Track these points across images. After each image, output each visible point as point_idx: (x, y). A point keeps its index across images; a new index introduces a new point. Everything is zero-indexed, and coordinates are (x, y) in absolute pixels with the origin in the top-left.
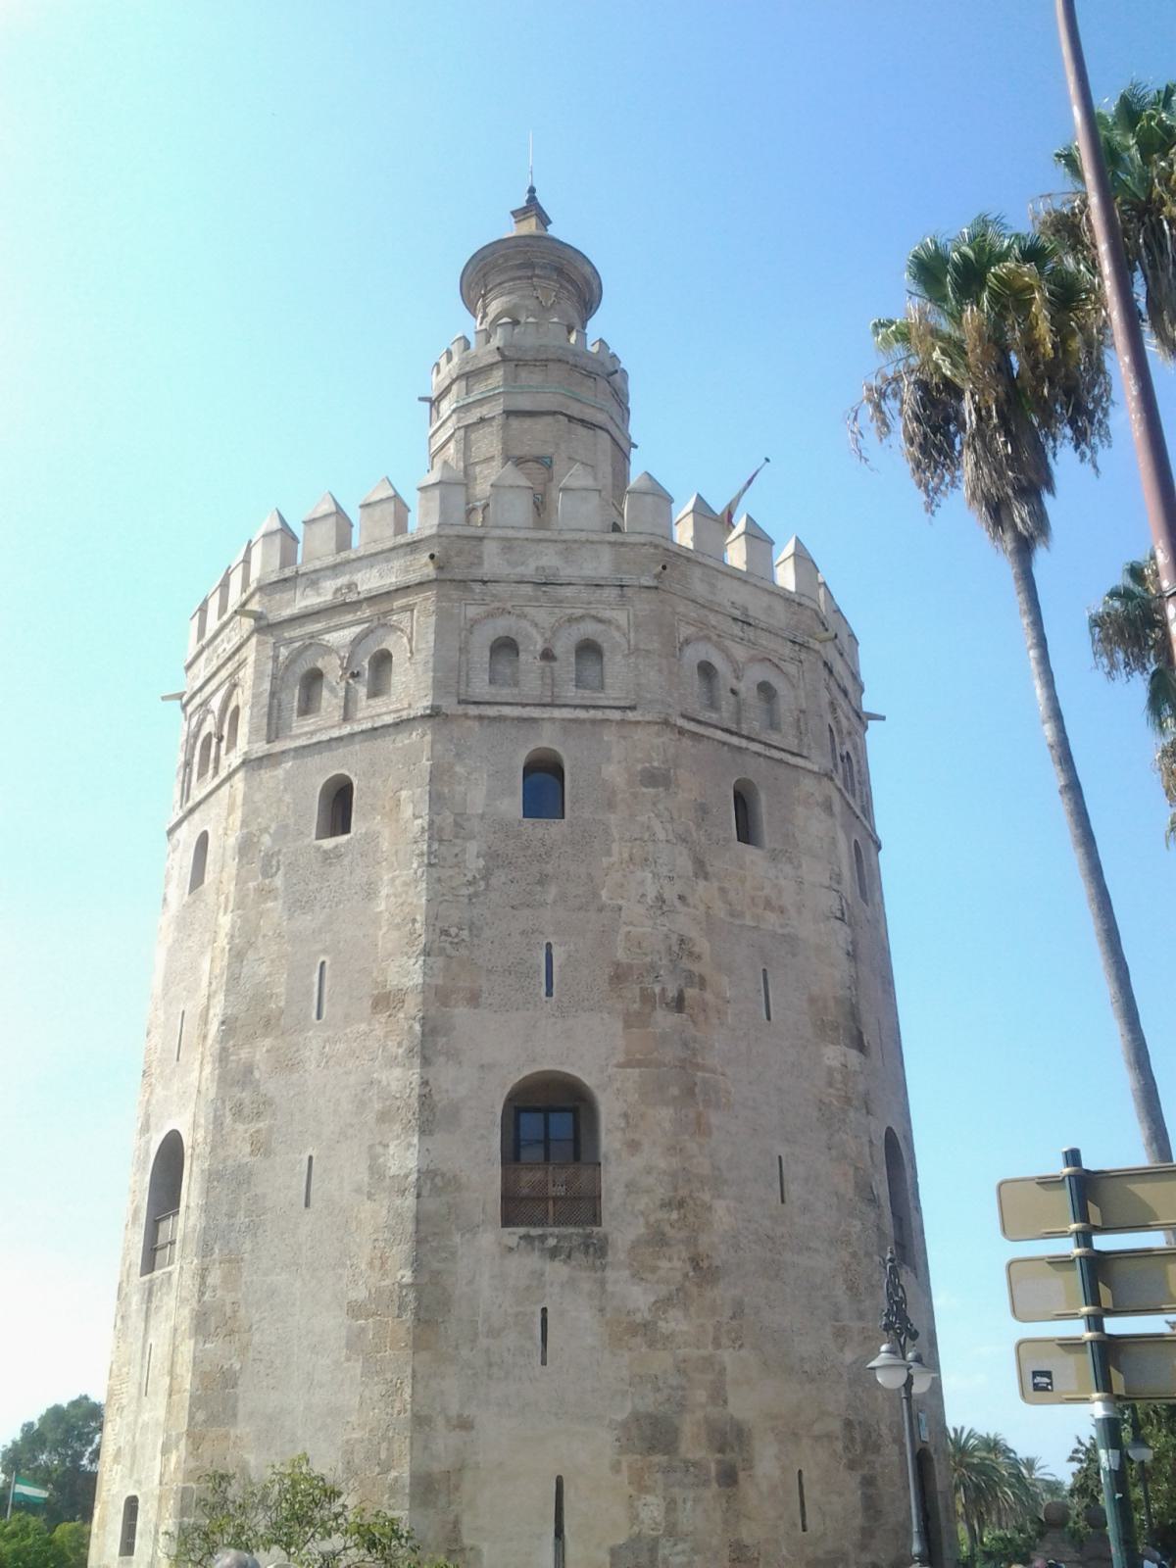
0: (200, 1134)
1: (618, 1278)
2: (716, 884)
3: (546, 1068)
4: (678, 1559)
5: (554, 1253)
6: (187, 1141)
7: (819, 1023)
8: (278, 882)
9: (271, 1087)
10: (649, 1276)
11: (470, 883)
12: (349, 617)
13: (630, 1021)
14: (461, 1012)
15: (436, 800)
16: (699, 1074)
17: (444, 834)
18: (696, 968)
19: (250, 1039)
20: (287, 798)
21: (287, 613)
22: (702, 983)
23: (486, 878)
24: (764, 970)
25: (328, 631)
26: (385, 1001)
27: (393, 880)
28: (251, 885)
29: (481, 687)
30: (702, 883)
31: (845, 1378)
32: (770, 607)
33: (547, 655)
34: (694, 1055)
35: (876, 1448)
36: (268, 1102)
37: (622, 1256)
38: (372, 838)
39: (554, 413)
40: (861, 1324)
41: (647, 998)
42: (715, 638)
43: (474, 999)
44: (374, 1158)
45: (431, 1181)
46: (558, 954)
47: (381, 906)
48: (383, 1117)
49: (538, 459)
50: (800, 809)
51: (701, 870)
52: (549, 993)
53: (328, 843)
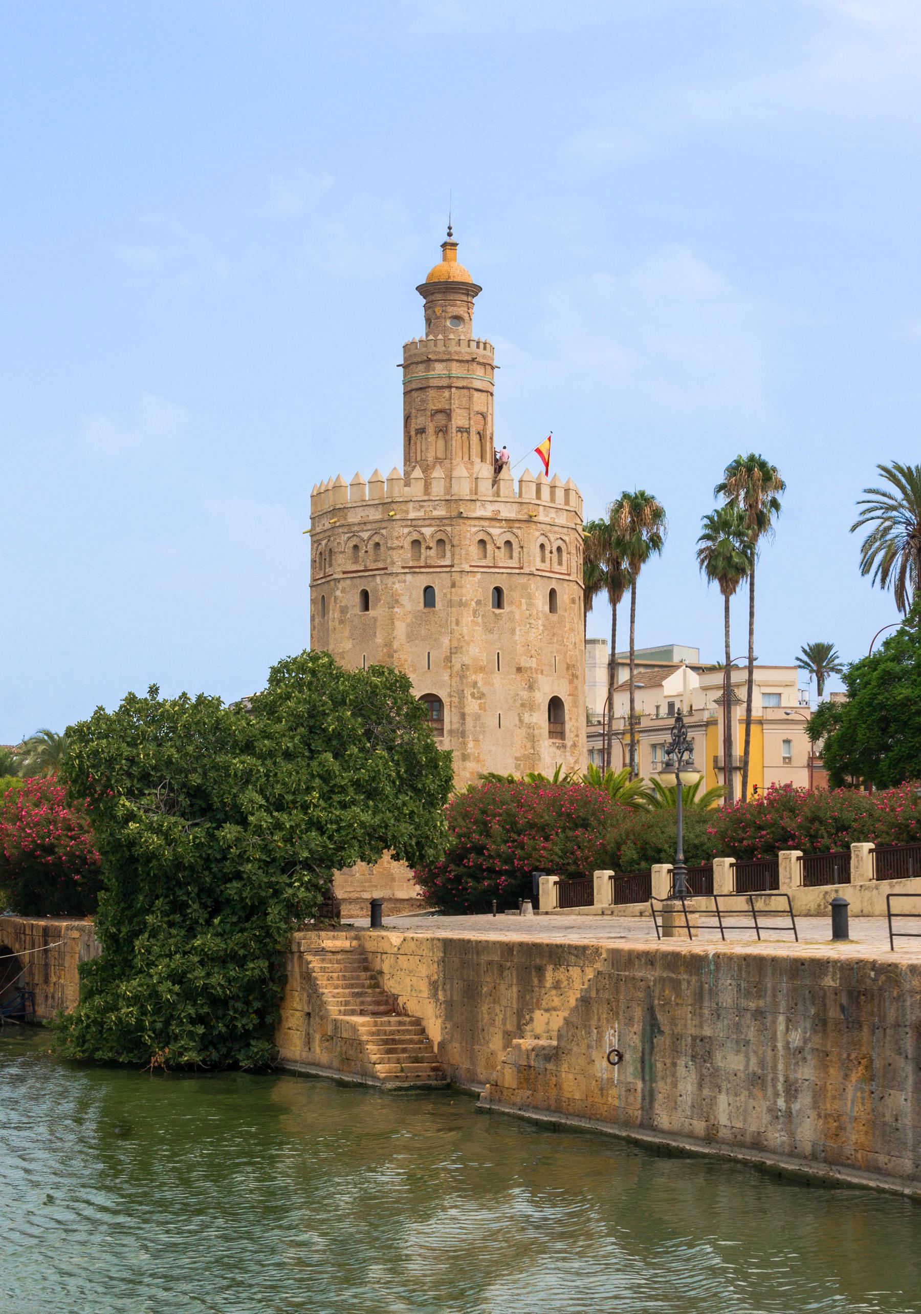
0: (456, 700)
1: (568, 754)
5: (558, 747)
6: (446, 700)
8: (480, 620)
9: (484, 689)
12: (498, 525)
13: (571, 682)
14: (539, 676)
19: (475, 672)
20: (480, 590)
21: (474, 515)
25: (490, 527)
26: (519, 670)
27: (520, 630)
28: (470, 619)
29: (539, 564)
33: (551, 552)
36: (483, 694)
38: (511, 612)
39: (487, 392)
41: (573, 675)
44: (520, 717)
47: (517, 638)
48: (523, 705)
49: (482, 414)
53: (497, 611)
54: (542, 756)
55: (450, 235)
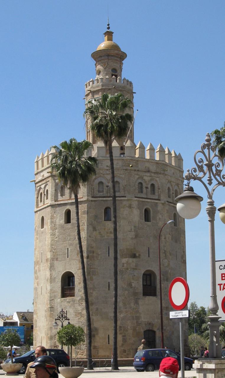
2: (98, 232)
3: (67, 271)
4: (83, 348)
7: (122, 255)
10: (81, 305)
11: (56, 238)
14: (55, 262)
15: (52, 222)
16: (92, 270)
17: (53, 229)
18: (92, 250)
22: (93, 252)
23: (59, 236)
24: (109, 247)
30: (95, 232)
31: (121, 319)
32: (117, 163)
34: (91, 266)
35: (127, 331)
37: (77, 302)
38: (45, 229)
40: (125, 310)
42: (102, 176)
43: (57, 259)
45: (52, 291)
46: (69, 249)
47: (46, 243)
50: (122, 209)
51: (95, 229)
52: (68, 257)
54: (56, 308)
55: (109, 28)
